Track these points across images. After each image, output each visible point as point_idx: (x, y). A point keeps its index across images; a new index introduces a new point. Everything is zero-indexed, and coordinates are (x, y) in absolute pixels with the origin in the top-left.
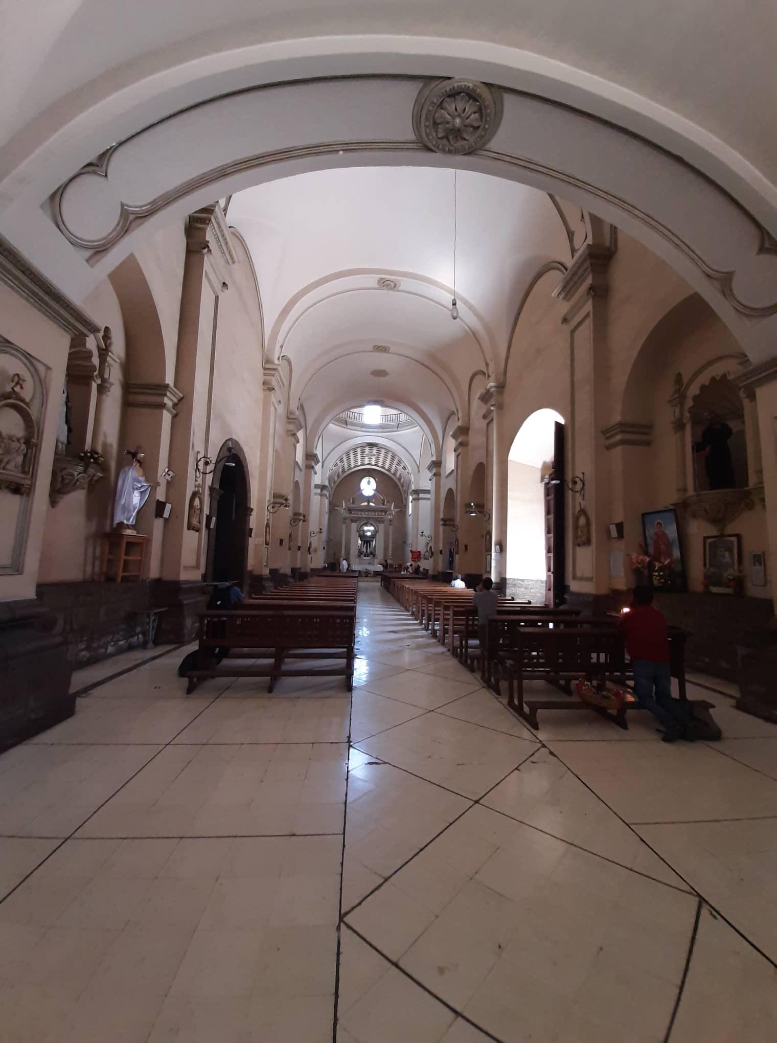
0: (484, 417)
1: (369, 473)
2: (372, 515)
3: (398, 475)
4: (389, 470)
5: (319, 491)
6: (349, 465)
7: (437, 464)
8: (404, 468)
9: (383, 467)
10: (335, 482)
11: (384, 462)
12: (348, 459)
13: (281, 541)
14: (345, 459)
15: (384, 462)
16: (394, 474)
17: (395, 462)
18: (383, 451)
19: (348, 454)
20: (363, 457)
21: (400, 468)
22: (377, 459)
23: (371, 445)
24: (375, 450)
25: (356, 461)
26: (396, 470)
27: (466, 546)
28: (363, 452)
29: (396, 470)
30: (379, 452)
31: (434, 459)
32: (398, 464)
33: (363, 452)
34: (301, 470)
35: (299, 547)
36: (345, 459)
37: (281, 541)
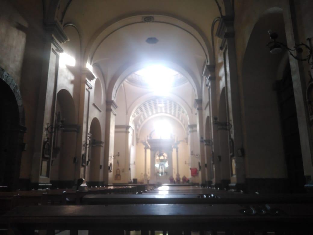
0: (221, 48)
7: (199, 102)
8: (183, 112)
13: (75, 159)
15: (170, 110)
27: (220, 157)
29: (179, 115)
31: (197, 98)
32: (179, 110)
34: (100, 111)
35: (101, 167)
36: (143, 109)
37: (75, 159)
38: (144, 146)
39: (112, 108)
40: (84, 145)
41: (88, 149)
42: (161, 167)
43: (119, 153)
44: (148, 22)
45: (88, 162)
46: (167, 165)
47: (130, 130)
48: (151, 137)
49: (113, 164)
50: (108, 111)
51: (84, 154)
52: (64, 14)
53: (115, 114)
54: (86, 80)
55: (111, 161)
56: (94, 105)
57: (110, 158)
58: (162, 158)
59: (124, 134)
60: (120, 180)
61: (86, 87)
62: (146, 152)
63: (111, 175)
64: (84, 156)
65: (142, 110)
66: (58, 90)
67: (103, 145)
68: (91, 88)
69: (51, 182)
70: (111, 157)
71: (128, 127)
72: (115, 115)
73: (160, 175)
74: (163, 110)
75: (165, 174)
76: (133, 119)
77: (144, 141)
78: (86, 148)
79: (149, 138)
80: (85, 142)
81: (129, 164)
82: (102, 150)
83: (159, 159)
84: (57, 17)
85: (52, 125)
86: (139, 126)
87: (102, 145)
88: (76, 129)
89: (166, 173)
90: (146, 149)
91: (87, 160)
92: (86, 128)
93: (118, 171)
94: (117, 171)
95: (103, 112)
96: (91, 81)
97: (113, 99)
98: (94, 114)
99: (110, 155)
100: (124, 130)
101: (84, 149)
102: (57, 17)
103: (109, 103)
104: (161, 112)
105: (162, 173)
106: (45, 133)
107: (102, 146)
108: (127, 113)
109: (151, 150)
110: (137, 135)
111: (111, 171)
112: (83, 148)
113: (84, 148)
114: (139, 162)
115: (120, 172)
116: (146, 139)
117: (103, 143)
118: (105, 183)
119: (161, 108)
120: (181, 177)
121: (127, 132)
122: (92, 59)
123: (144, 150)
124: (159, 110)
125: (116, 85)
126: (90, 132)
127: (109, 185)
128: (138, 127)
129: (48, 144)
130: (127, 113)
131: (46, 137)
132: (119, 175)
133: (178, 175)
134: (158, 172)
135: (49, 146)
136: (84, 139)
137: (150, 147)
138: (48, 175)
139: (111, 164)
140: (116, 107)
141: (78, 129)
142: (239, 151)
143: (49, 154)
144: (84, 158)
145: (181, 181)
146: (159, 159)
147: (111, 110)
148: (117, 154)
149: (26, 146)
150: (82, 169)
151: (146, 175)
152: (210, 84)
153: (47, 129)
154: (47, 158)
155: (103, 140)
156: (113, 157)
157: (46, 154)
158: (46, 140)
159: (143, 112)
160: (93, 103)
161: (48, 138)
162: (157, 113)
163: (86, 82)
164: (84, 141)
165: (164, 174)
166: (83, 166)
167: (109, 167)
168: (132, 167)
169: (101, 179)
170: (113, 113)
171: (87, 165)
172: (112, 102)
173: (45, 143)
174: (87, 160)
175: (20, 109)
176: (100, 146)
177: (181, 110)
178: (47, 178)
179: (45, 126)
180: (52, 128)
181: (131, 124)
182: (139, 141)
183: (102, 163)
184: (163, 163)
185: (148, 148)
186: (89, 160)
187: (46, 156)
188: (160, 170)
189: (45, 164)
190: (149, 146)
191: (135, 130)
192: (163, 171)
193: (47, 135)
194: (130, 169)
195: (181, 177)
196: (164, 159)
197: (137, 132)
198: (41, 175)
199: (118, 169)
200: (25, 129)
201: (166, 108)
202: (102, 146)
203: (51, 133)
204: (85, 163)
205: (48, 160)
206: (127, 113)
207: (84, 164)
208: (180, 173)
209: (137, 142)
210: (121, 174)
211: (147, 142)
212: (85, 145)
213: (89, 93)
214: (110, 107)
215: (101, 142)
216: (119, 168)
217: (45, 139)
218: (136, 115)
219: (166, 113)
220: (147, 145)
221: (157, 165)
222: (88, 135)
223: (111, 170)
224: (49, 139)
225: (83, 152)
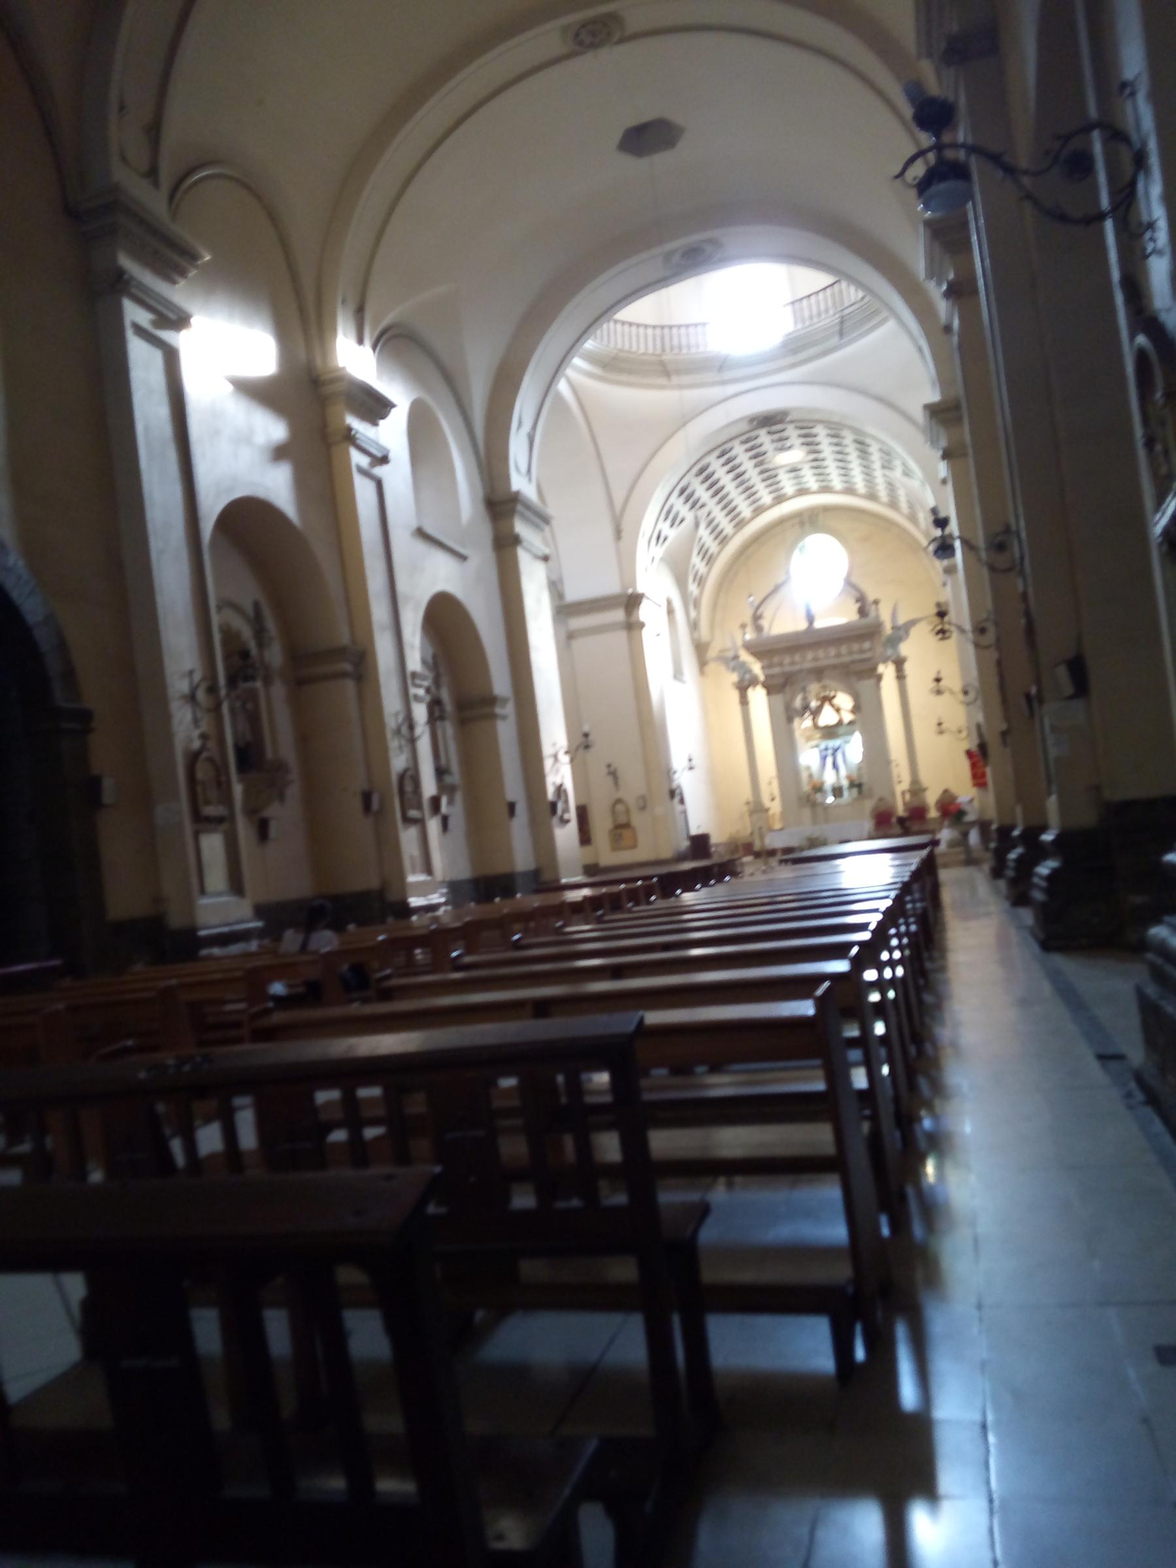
1: (809, 521)
2: (827, 656)
3: (903, 505)
4: (872, 496)
5: (619, 615)
6: (730, 510)
9: (850, 491)
10: (701, 581)
11: (845, 472)
12: (717, 490)
13: (367, 798)
14: (702, 492)
15: (845, 472)
16: (893, 504)
17: (876, 457)
18: (821, 432)
19: (705, 474)
20: (769, 476)
21: (897, 474)
22: (817, 464)
23: (770, 421)
24: (792, 432)
25: (749, 492)
26: (891, 487)
28: (758, 456)
29: (891, 487)
30: (810, 442)
32: (887, 466)
33: (758, 456)
35: (511, 807)
37: (367, 798)
38: (734, 677)
39: (520, 528)
40: (398, 732)
42: (829, 760)
43: (586, 735)
44: (594, 46)
46: (854, 749)
47: (644, 612)
48: (759, 629)
49: (569, 786)
50: (505, 545)
51: (406, 770)
52: (154, 130)
53: (540, 554)
54: (350, 429)
55: (559, 774)
56: (421, 534)
57: (548, 763)
58: (828, 717)
59: (620, 637)
60: (634, 846)
61: (357, 458)
62: (744, 701)
63: (566, 836)
64: (411, 776)
65: (695, 505)
66: (211, 507)
68: (384, 460)
69: (260, 911)
70: (555, 757)
71: (632, 602)
72: (546, 559)
73: (830, 799)
74: (811, 482)
75: (855, 791)
76: (659, 551)
77: (731, 654)
78: (413, 741)
79: (749, 636)
80: (401, 718)
81: (669, 773)
82: (506, 731)
83: (816, 726)
84: (124, 159)
86: (701, 581)
87: (498, 710)
88: (347, 667)
89: (856, 785)
90: (743, 688)
92: (401, 651)
93: (620, 807)
94: (613, 812)
95: (482, 557)
96: (375, 424)
97: (518, 483)
98: (429, 575)
99: (547, 750)
100: (619, 615)
101: (400, 747)
102: (124, 159)
103: (500, 506)
104: (802, 492)
105: (837, 791)
107: (504, 718)
108: (618, 533)
109: (771, 688)
110: (694, 626)
111: (564, 822)
112: (393, 744)
113: (403, 742)
114: (713, 752)
115: (628, 811)
116: (739, 643)
117: (505, 701)
118: (543, 880)
119: (794, 470)
120: (932, 798)
121: (633, 627)
122: (359, 313)
123: (735, 695)
124: (788, 485)
125: (524, 406)
127: (564, 881)
128: (693, 588)
130: (618, 533)
132: (627, 825)
133: (917, 789)
134: (818, 788)
136: (391, 702)
137: (762, 678)
138: (236, 886)
139: (560, 790)
140: (541, 519)
141: (360, 662)
142: (1062, 672)
144: (409, 788)
145: (933, 813)
146: (816, 726)
147: (516, 540)
148: (581, 739)
149: (108, 785)
150: (408, 838)
151: (757, 808)
152: (956, 323)
153: (192, 698)
155: (501, 684)
156: (565, 759)
157: (207, 802)
159: (705, 510)
160: (414, 524)
161: (204, 737)
162: (780, 499)
163: (349, 437)
164: (397, 714)
165: (846, 793)
166: (408, 821)
167: (553, 806)
168: (685, 780)
169: (522, 859)
170: (528, 550)
172: (515, 499)
173: (193, 758)
176: (493, 717)
177: (897, 463)
179: (178, 685)
180: (212, 689)
181: (654, 583)
182: (712, 653)
183: (513, 789)
184: (836, 743)
185: (754, 682)
187: (210, 810)
188: (830, 778)
189: (213, 845)
190: (757, 668)
191: (678, 605)
192: (845, 783)
193: (196, 722)
194: (674, 793)
195: (932, 798)
196: (840, 723)
197: (693, 614)
198: (203, 891)
199: (619, 801)
201: (817, 464)
202: (504, 718)
203: (216, 709)
205: (225, 826)
206: (620, 531)
208: (925, 778)
209: (702, 663)
210: (637, 819)
211: (745, 657)
212: (404, 730)
213: (379, 484)
214: (512, 527)
215: (491, 700)
216: (620, 794)
217: (191, 740)
218: (672, 533)
219: (826, 489)
220: (749, 671)
221: (809, 757)
223: (566, 816)
225: (399, 762)
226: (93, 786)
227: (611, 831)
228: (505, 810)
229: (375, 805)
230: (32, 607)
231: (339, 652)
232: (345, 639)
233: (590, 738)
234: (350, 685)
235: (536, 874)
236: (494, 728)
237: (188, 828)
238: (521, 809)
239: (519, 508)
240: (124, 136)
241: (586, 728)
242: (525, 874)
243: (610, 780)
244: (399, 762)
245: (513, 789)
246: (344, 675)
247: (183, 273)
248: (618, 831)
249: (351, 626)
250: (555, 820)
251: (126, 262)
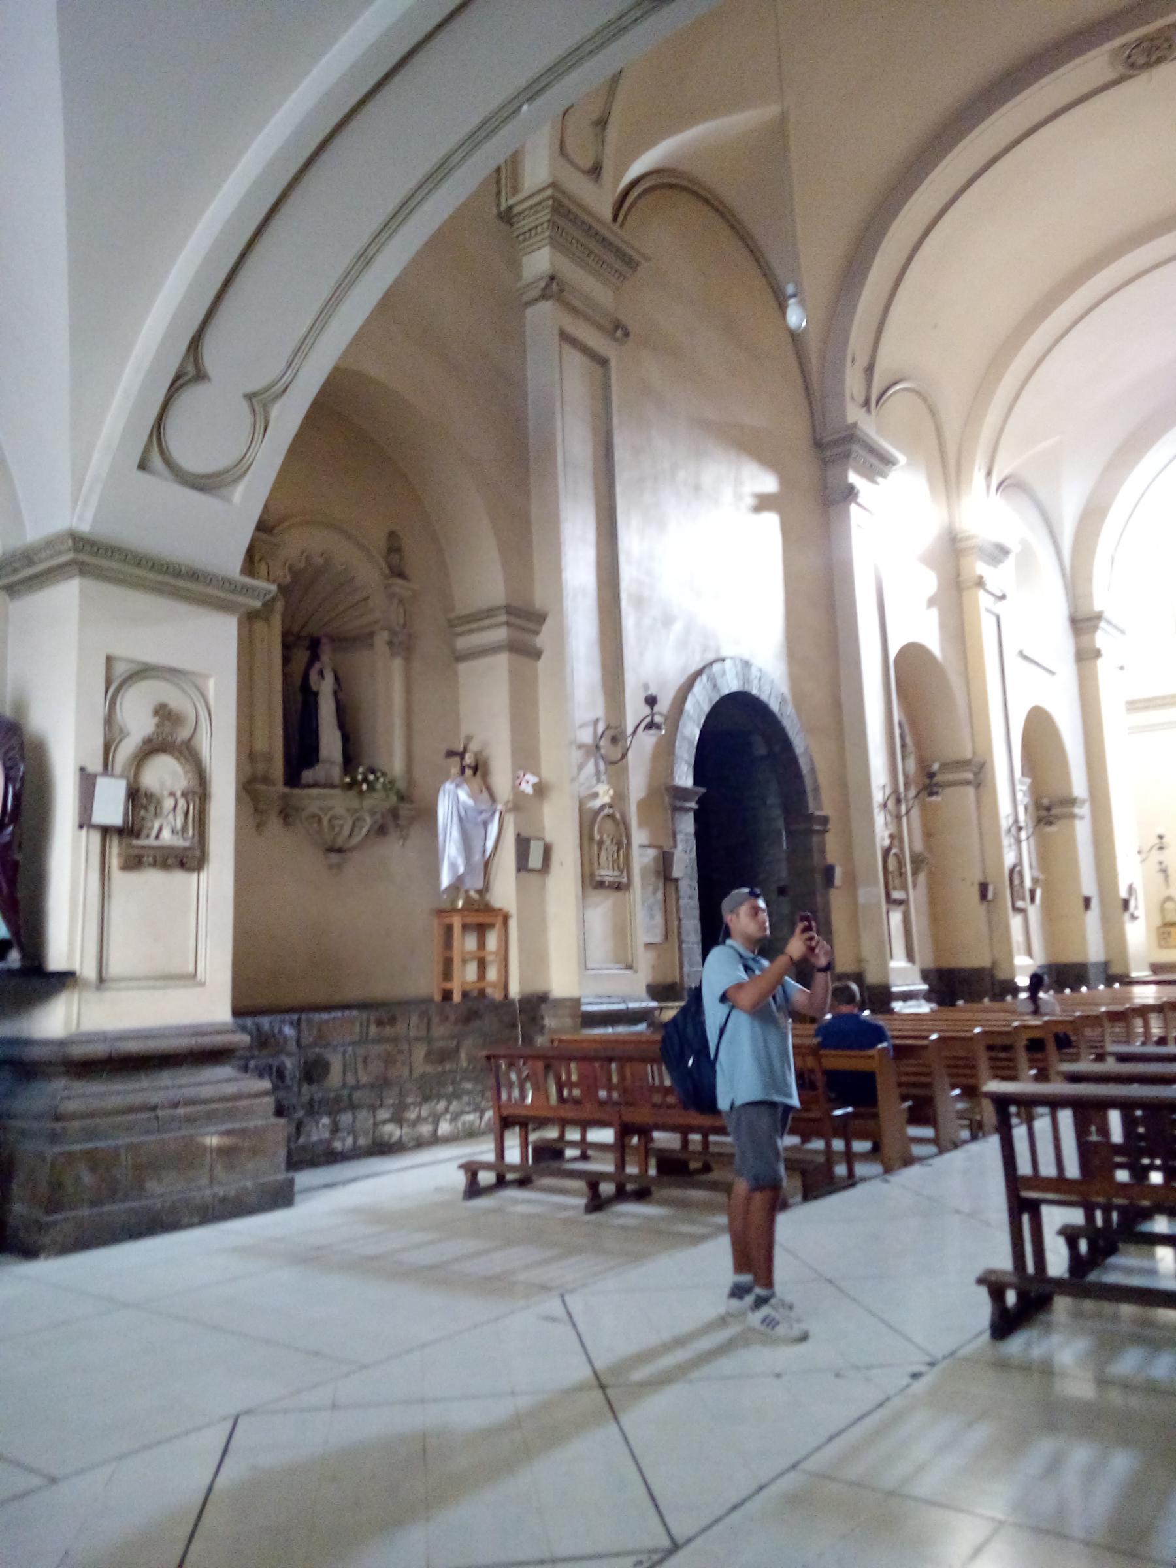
13: (983, 889)
35: (1087, 902)
37: (983, 889)
41: (1024, 845)
43: (1161, 837)
45: (1032, 893)
49: (1139, 887)
50: (1086, 656)
52: (870, 370)
64: (1015, 872)
67: (1084, 810)
69: (925, 976)
78: (1018, 841)
80: (1011, 820)
82: (1082, 830)
85: (895, 791)
87: (1077, 811)
88: (970, 776)
91: (1028, 883)
94: (1162, 910)
101: (1010, 846)
106: (880, 819)
107: (1082, 818)
112: (1007, 841)
117: (1083, 802)
126: (1023, 774)
129: (895, 854)
131: (886, 834)
135: (900, 860)
138: (910, 957)
141: (977, 773)
143: (904, 887)
144: (1016, 882)
149: (838, 871)
150: (1016, 922)
154: (900, 902)
155: (1079, 787)
157: (895, 888)
158: (887, 842)
161: (891, 836)
164: (1008, 816)
166: (1016, 910)
167: (1126, 904)
169: (1094, 952)
171: (1033, 899)
174: (1028, 883)
175: (803, 763)
176: (1073, 816)
178: (909, 965)
179: (878, 796)
186: (1035, 881)
187: (897, 895)
189: (896, 918)
193: (886, 824)
198: (891, 957)
200: (825, 820)
202: (1082, 818)
203: (898, 817)
204: (1023, 899)
205: (902, 908)
207: (1020, 904)
212: (1014, 830)
215: (1072, 802)
217: (883, 839)
222: (1018, 787)
223: (1136, 913)
224: (896, 837)
225: (1009, 859)
226: (829, 872)
227: (1158, 928)
228: (1081, 904)
229: (990, 895)
230: (799, 743)
231: (963, 764)
232: (969, 755)
233: (1165, 840)
234: (971, 791)
235: (1106, 965)
236: (1073, 830)
237: (884, 906)
238: (1094, 903)
239: (1102, 624)
240: (853, 382)
241: (1161, 832)
242: (1096, 965)
243: (1161, 876)
244: (1009, 859)
245: (1088, 887)
246: (967, 783)
247: (884, 475)
248: (1167, 929)
249: (973, 741)
250: (1127, 916)
251: (853, 478)
